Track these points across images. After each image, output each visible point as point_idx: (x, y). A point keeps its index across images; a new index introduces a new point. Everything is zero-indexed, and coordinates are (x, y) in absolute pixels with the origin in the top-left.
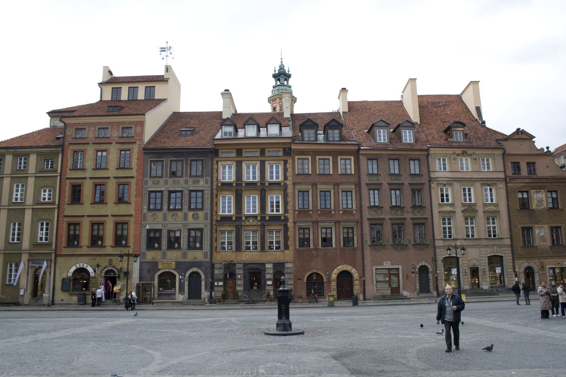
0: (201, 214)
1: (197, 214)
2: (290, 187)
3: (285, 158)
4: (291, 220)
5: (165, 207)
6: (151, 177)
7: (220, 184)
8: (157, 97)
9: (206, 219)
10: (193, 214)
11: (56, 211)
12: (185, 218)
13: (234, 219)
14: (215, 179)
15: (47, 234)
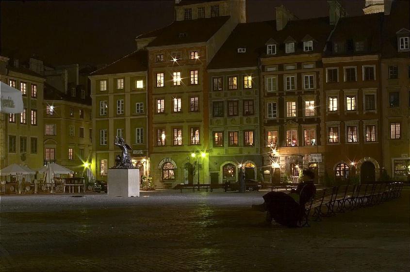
0: (252, 118)
1: (250, 119)
2: (322, 93)
3: (317, 70)
4: (322, 121)
5: (226, 114)
6: (214, 90)
7: (266, 95)
8: (221, 14)
9: (256, 121)
10: (247, 119)
11: (147, 119)
12: (241, 122)
13: (278, 121)
14: (262, 91)
15: (142, 138)
